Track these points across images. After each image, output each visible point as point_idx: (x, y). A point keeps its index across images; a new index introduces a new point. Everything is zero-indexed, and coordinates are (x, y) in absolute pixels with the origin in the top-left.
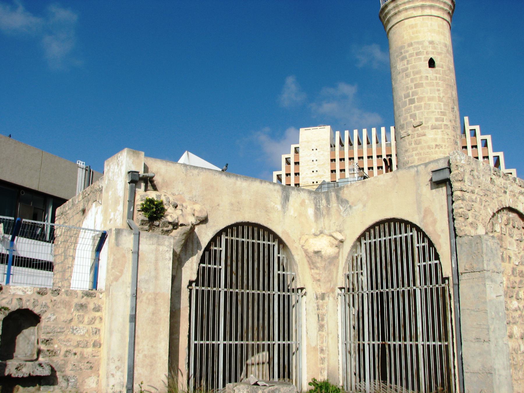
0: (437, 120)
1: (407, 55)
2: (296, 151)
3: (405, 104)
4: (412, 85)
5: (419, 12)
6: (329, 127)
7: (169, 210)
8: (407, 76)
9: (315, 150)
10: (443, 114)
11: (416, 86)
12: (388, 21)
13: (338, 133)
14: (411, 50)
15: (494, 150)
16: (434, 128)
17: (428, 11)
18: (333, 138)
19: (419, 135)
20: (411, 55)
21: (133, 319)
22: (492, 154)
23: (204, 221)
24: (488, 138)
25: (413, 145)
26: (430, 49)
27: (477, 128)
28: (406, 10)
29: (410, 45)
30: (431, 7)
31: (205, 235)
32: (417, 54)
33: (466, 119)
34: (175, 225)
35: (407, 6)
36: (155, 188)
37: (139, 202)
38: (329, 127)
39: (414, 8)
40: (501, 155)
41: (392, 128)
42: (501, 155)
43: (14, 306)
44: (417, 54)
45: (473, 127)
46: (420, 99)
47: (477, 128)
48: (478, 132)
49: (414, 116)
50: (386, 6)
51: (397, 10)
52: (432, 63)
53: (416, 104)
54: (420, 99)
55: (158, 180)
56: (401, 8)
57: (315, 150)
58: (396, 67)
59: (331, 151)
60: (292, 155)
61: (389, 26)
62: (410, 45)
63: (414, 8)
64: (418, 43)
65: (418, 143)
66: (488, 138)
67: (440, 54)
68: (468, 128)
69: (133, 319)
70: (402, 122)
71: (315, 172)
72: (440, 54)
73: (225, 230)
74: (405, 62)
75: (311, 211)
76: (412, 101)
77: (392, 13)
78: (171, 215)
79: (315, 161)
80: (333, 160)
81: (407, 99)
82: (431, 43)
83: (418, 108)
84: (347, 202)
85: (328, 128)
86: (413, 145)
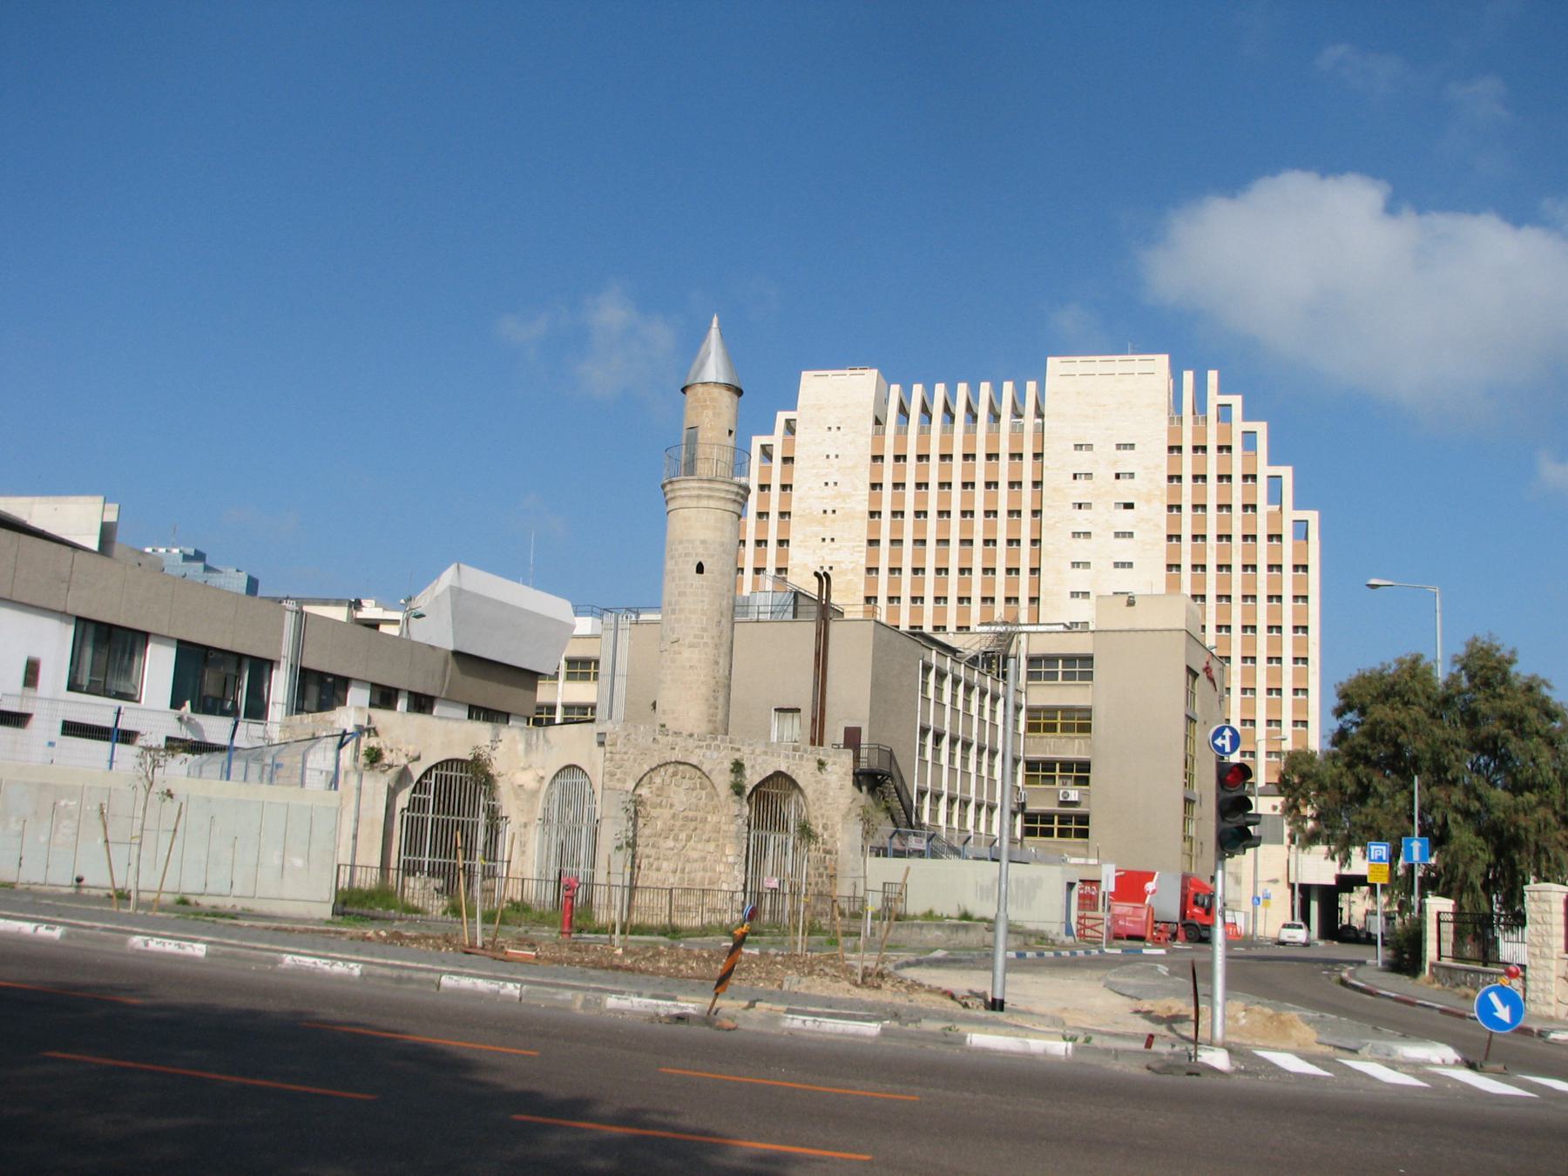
0: (695, 636)
2: (790, 427)
5: (694, 503)
6: (875, 372)
7: (386, 753)
9: (834, 429)
10: (704, 630)
11: (680, 594)
13: (895, 389)
14: (680, 547)
15: (1272, 461)
16: (691, 646)
17: (704, 503)
18: (882, 401)
21: (355, 837)
22: (1264, 470)
23: (418, 758)
26: (700, 550)
27: (1236, 401)
29: (681, 542)
30: (709, 497)
31: (417, 771)
33: (1213, 377)
34: (390, 766)
36: (377, 734)
37: (363, 748)
38: (875, 372)
39: (690, 497)
41: (1031, 386)
45: (1225, 399)
46: (681, 610)
47: (1236, 401)
48: (1237, 411)
49: (673, 630)
52: (700, 569)
54: (681, 610)
55: (379, 727)
57: (834, 429)
59: (877, 433)
60: (777, 439)
61: (670, 507)
63: (690, 497)
65: (673, 661)
67: (712, 556)
68: (1214, 399)
69: (355, 837)
71: (831, 484)
72: (712, 556)
73: (435, 766)
75: (521, 747)
76: (673, 612)
78: (388, 758)
79: (832, 456)
80: (877, 458)
82: (703, 542)
83: (678, 621)
85: (871, 376)
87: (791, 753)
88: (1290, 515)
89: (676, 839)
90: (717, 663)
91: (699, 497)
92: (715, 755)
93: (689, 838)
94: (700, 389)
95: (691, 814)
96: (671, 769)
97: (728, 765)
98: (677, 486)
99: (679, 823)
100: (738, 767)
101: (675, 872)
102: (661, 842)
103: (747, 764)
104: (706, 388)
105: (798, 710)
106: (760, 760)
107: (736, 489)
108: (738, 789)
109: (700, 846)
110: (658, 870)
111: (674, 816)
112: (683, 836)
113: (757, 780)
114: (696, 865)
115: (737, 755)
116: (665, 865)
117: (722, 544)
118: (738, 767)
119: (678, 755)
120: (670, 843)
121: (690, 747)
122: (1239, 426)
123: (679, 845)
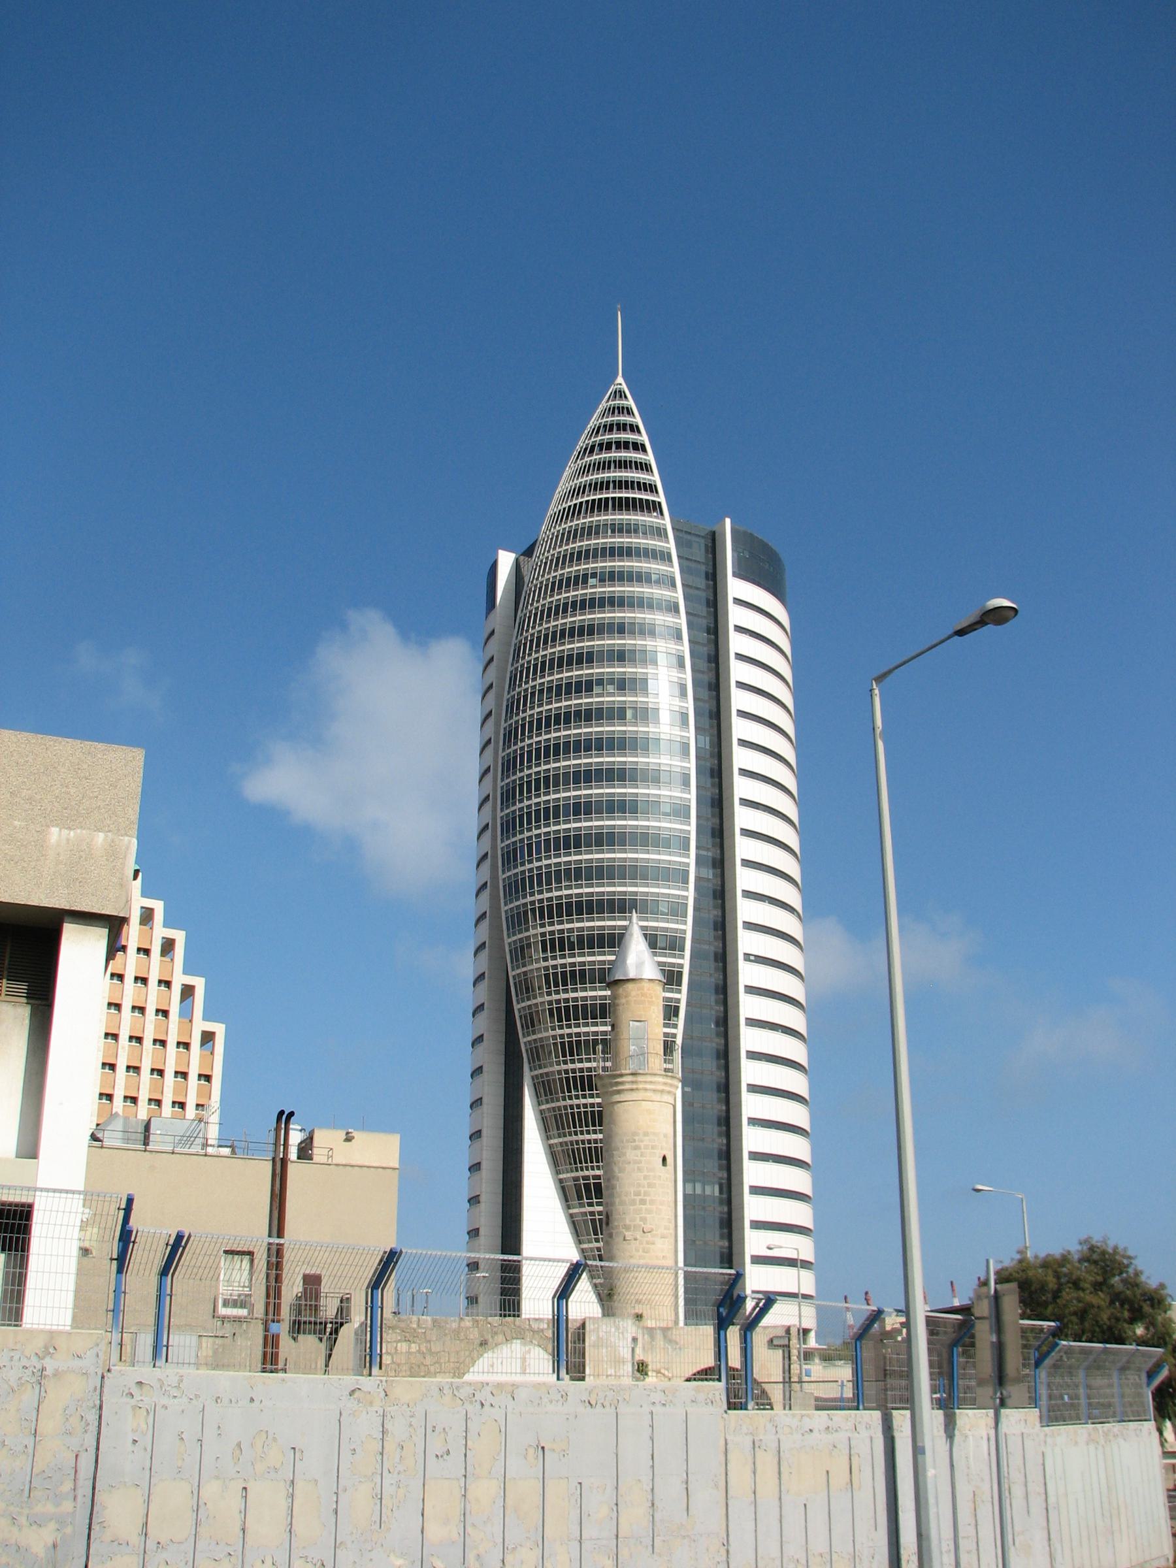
1: (642, 1145)
3: (633, 1202)
4: (645, 1182)
5: (657, 1097)
8: (639, 1169)
11: (649, 1185)
12: (619, 1092)
19: (648, 1243)
20: (646, 1147)
24: (179, 936)
25: (641, 1253)
27: (158, 906)
28: (646, 1090)
29: (646, 1134)
32: (653, 1147)
35: (648, 1086)
40: (199, 983)
42: (199, 983)
44: (653, 1147)
46: (652, 1202)
47: (158, 906)
48: (159, 916)
49: (644, 1220)
50: (621, 1075)
51: (634, 1086)
52: (664, 1159)
53: (648, 1206)
54: (652, 1202)
56: (641, 1086)
58: (625, 1154)
62: (646, 1134)
64: (654, 1134)
66: (179, 936)
70: (628, 1222)
74: (638, 1152)
76: (643, 1202)
77: (627, 1086)
81: (638, 1198)
83: (649, 1211)
84: (677, 1343)
86: (641, 1253)
88: (200, 1025)
91: (662, 1091)
94: (646, 985)
98: (640, 1078)
104: (652, 984)
105: (251, 1254)
122: (160, 932)
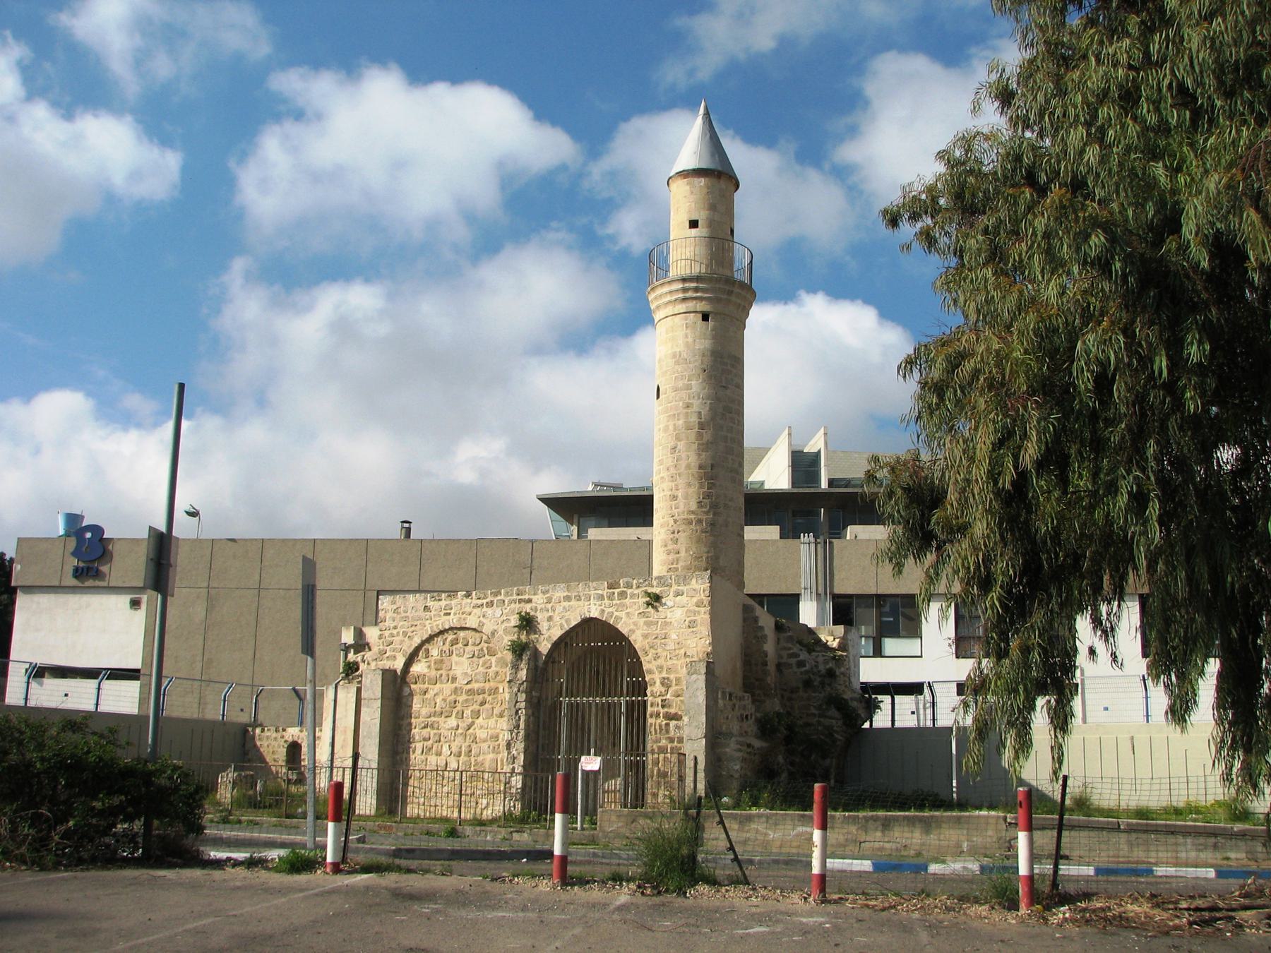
43: (290, 740)
87: (606, 592)
89: (461, 715)
90: (675, 498)
92: (498, 612)
93: (477, 714)
95: (475, 686)
96: (450, 637)
97: (514, 621)
99: (461, 698)
100: (528, 623)
101: (459, 756)
102: (441, 720)
103: (541, 617)
106: (559, 609)
107: (680, 286)
108: (519, 650)
109: (492, 722)
110: (439, 754)
111: (456, 691)
112: (468, 712)
113: (557, 633)
114: (484, 746)
115: (527, 608)
116: (445, 749)
117: (674, 356)
118: (528, 623)
119: (453, 621)
120: (452, 722)
121: (468, 609)
123: (463, 725)
